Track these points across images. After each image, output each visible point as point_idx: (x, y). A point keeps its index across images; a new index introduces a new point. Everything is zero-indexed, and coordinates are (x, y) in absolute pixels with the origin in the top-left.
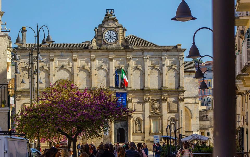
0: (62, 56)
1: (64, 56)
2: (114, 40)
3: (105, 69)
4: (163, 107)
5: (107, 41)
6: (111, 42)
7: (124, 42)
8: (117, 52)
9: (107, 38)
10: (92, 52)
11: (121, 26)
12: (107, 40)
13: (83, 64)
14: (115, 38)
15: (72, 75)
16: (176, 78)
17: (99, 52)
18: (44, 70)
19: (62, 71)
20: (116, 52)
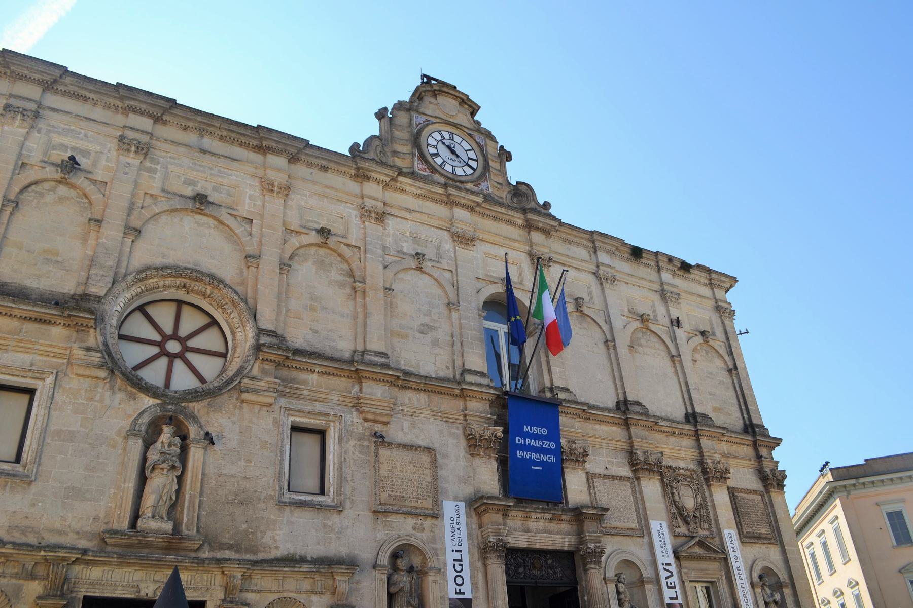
0: (204, 151)
1: (214, 154)
2: (469, 171)
3: (436, 276)
4: (718, 511)
5: (440, 166)
6: (454, 173)
7: (509, 196)
8: (488, 216)
9: (438, 154)
10: (368, 178)
11: (489, 135)
12: (439, 160)
13: (320, 224)
14: (474, 164)
15: (251, 259)
16: (728, 388)
17: (404, 196)
18: (63, 190)
19: (189, 224)
20: (483, 215)
